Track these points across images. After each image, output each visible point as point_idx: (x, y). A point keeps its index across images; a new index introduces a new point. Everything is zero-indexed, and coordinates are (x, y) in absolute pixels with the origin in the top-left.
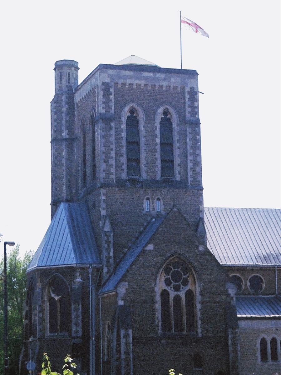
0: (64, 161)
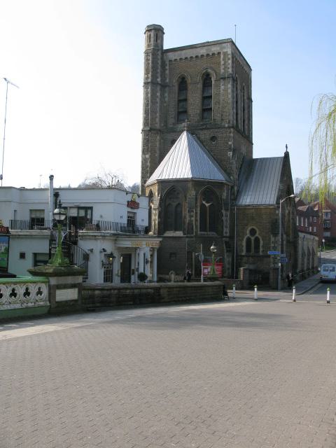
0: (158, 100)
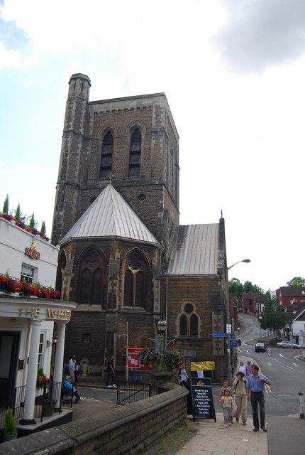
0: (79, 152)
